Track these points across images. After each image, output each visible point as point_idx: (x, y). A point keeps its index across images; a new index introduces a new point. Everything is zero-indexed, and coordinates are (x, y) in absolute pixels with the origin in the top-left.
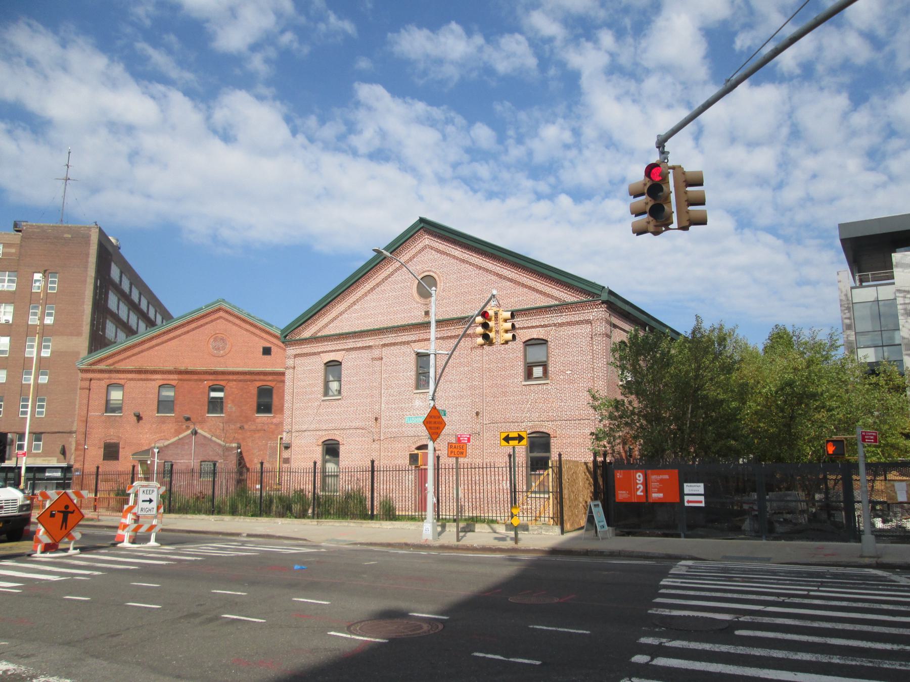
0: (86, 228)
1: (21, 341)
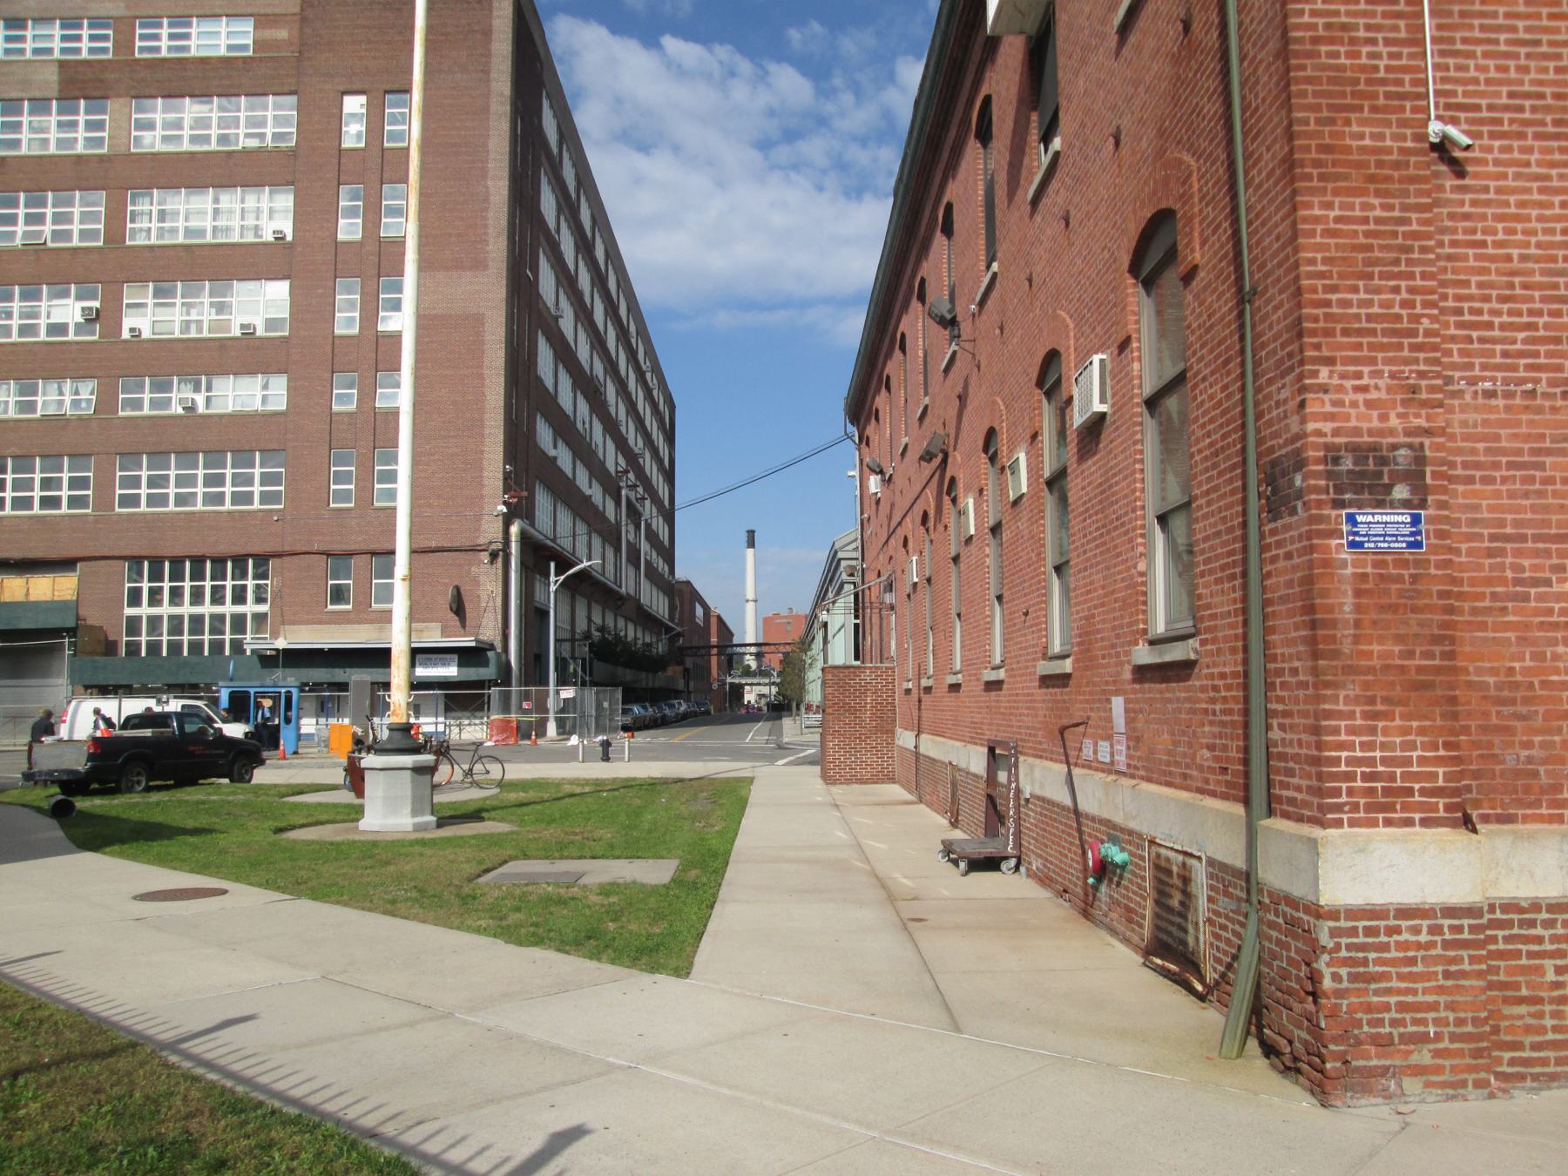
1: (320, 291)
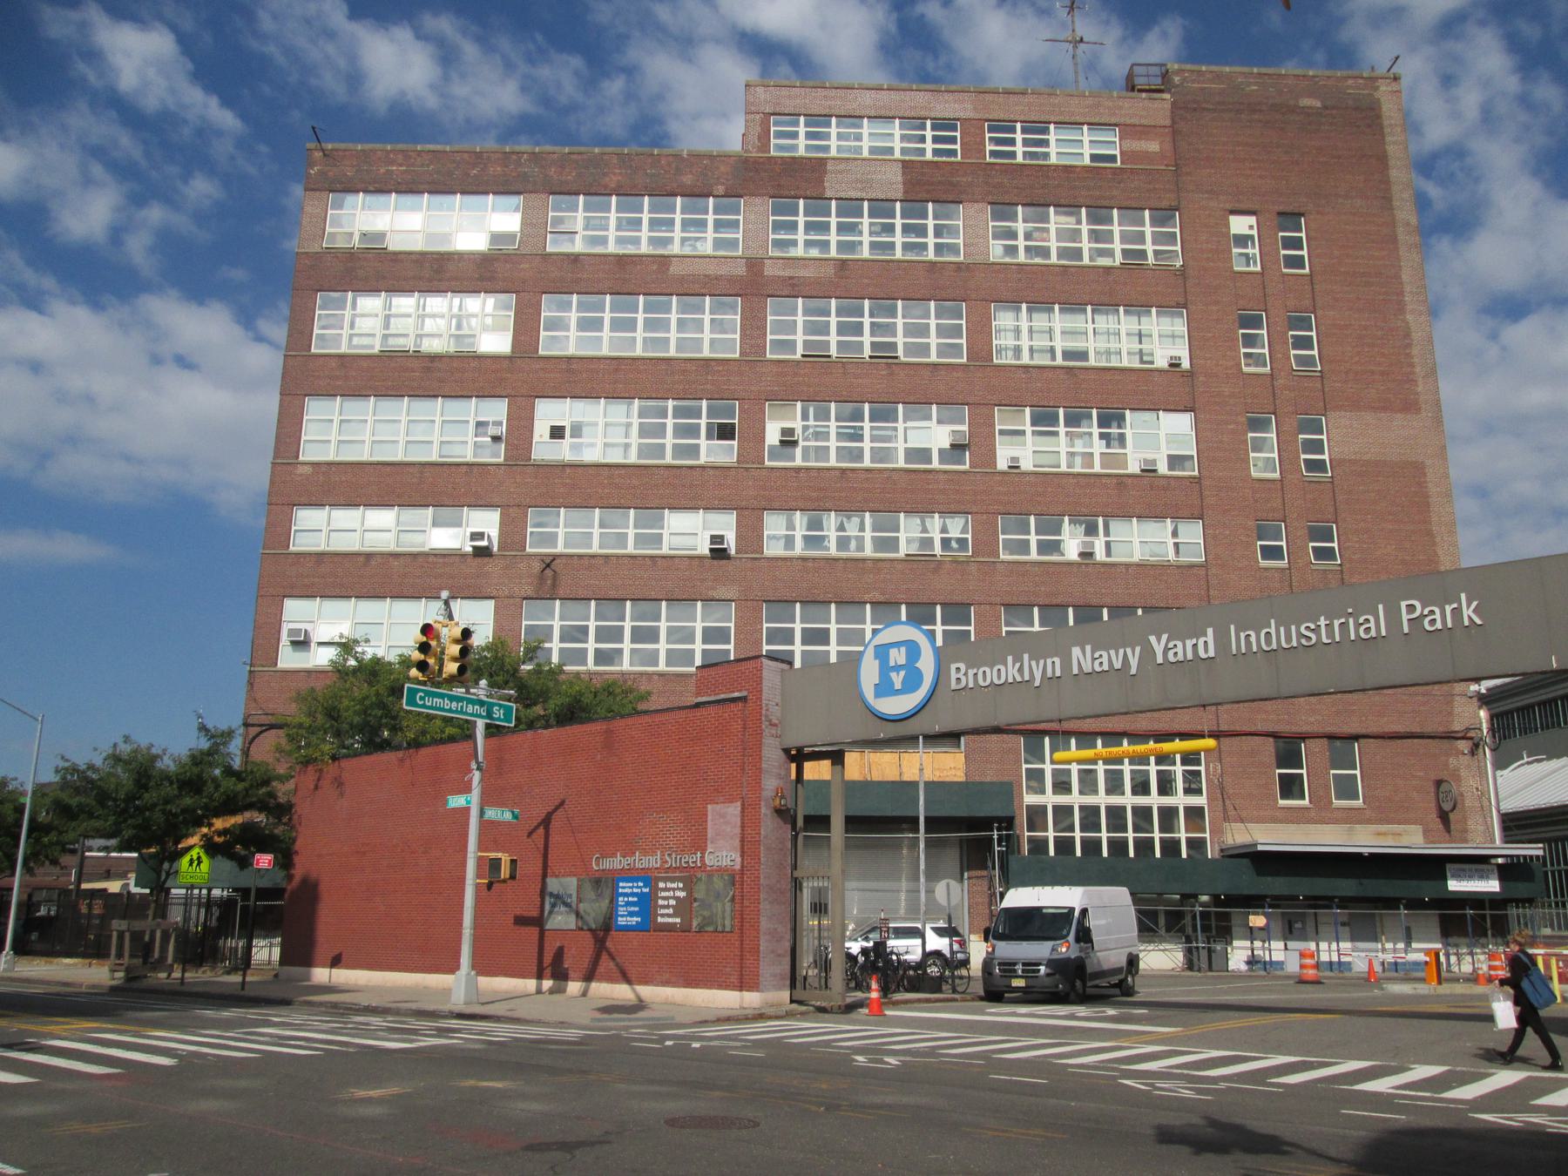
0: (1361, 81)
1: (1232, 427)
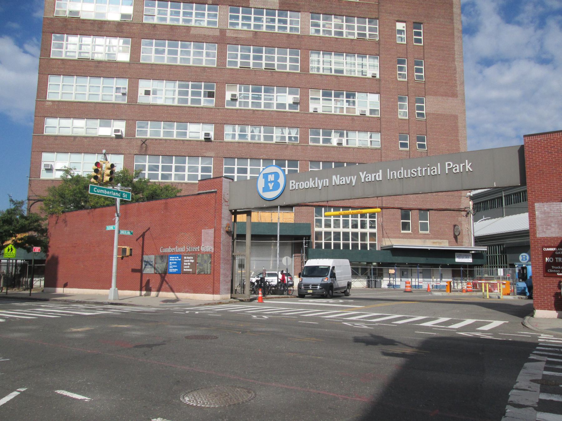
1: (392, 100)
